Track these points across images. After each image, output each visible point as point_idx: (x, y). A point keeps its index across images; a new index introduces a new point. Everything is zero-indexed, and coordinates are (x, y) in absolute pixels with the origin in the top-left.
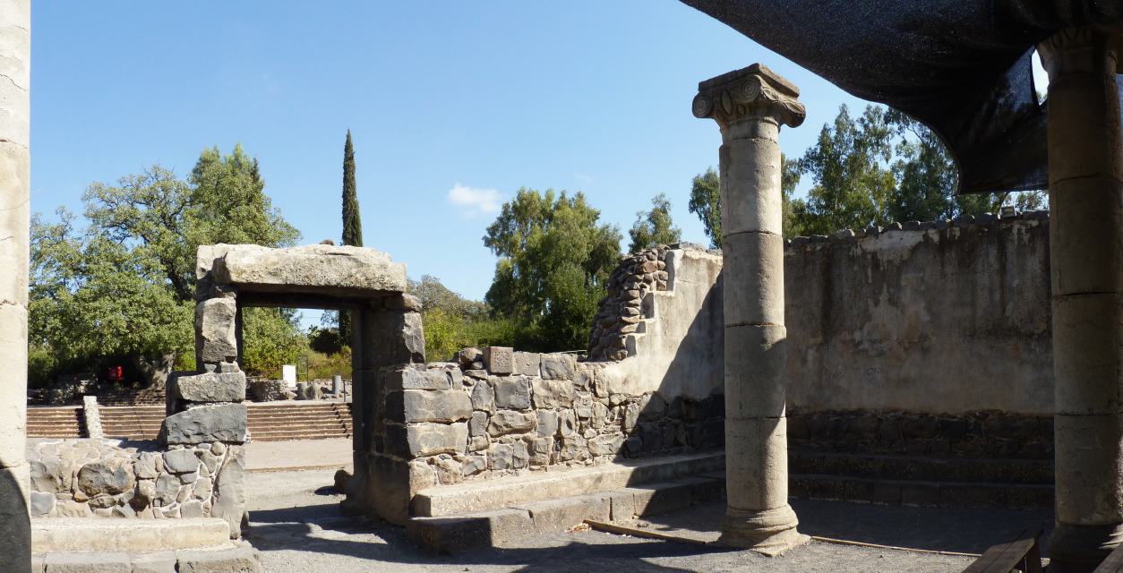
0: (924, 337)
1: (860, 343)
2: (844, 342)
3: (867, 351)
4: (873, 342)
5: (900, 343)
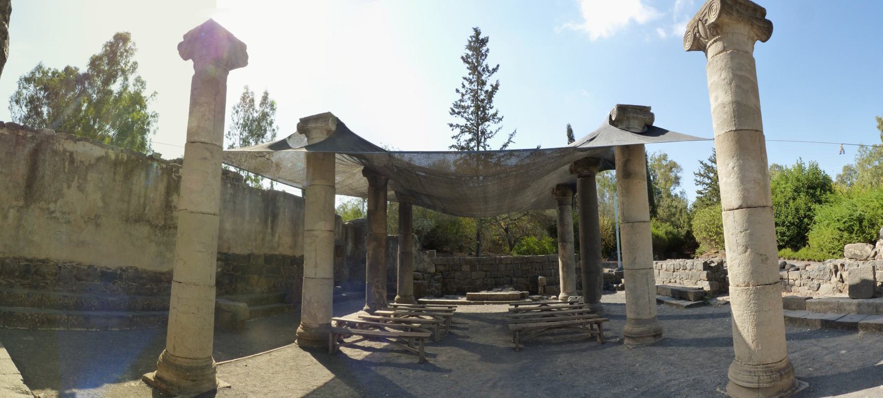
0: (97, 217)
1: (53, 212)
2: (42, 209)
3: (58, 218)
4: (64, 213)
5: (82, 217)
